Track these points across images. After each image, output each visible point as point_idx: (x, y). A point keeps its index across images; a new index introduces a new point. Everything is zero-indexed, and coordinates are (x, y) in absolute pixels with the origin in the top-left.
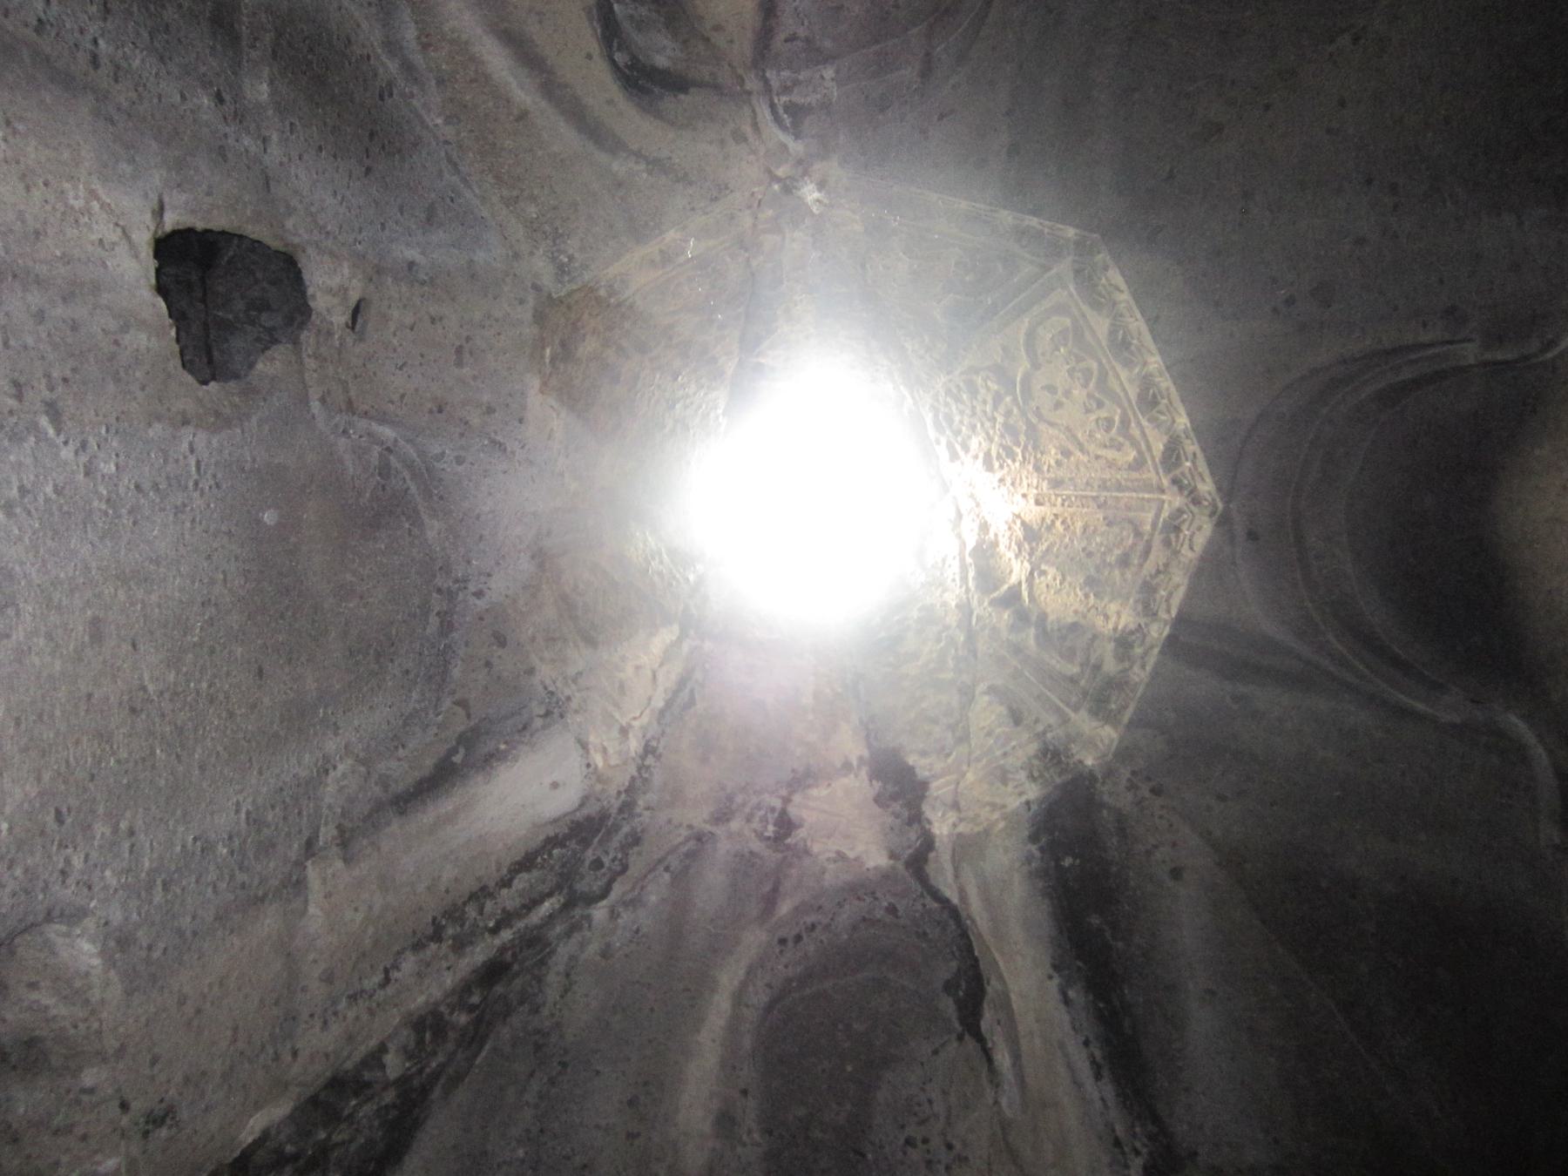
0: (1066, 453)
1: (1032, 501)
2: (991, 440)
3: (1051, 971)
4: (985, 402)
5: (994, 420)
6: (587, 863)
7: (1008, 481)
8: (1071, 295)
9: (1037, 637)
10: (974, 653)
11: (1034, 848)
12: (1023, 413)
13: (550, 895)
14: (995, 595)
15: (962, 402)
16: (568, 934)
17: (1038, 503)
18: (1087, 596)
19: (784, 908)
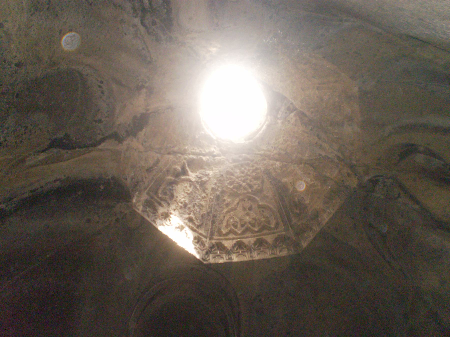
0: (228, 205)
1: (214, 186)
2: (237, 178)
3: (67, 176)
4: (251, 181)
5: (244, 182)
6: (156, 20)
7: (222, 179)
8: (281, 231)
9: (171, 180)
10: (169, 153)
11: (110, 177)
12: (244, 194)
13: (150, 4)
14: (187, 166)
15: (252, 173)
16: (134, 8)
17: (213, 189)
18: (182, 203)
19: (114, 86)
